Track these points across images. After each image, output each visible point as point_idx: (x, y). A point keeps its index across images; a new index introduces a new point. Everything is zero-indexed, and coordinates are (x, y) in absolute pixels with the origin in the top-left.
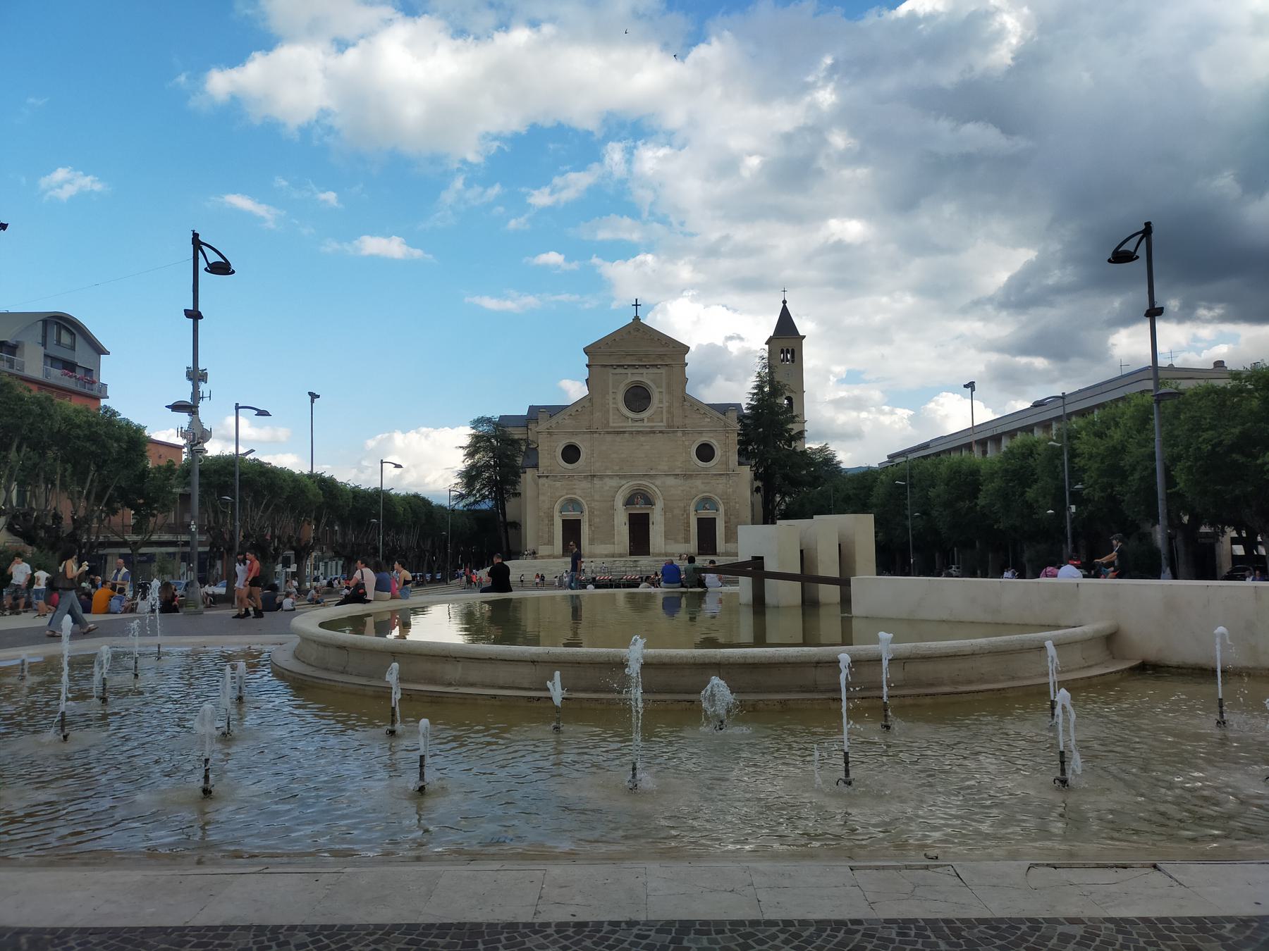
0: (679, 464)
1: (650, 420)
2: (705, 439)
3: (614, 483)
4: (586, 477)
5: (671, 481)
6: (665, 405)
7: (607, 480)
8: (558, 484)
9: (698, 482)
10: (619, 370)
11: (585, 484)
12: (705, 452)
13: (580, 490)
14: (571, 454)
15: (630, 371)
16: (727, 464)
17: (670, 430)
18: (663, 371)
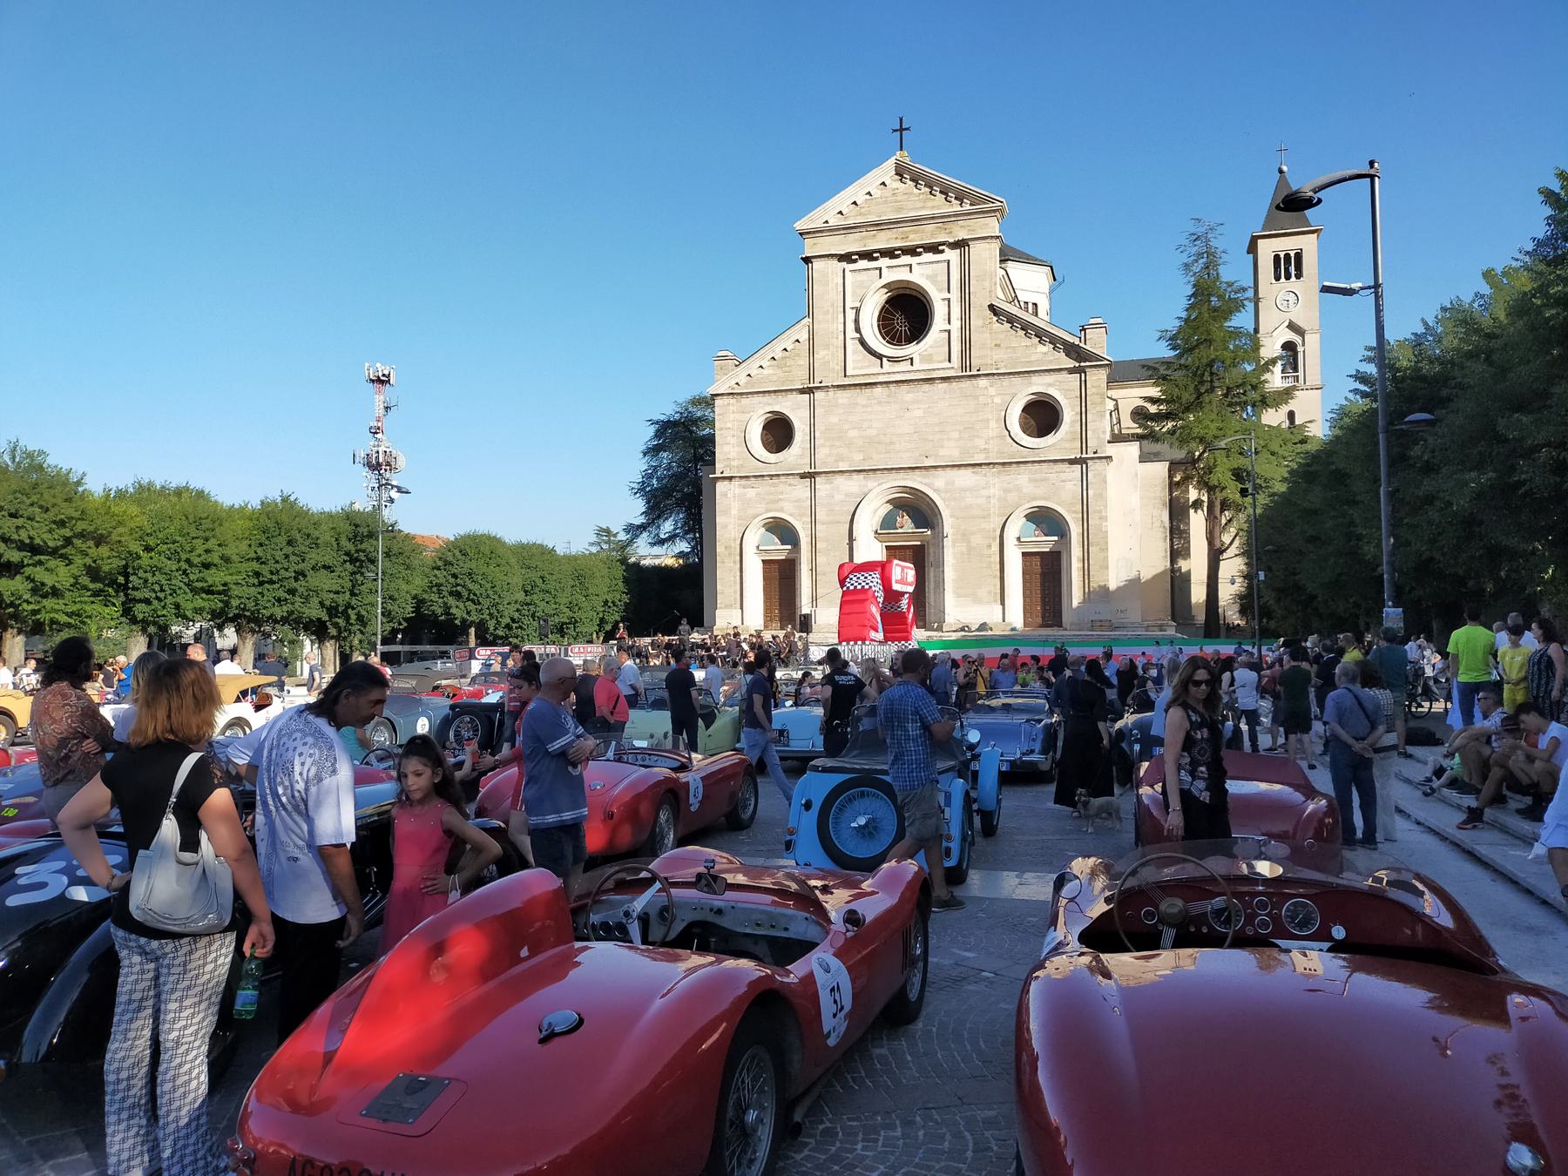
0: (980, 443)
1: (927, 358)
2: (1040, 385)
3: (853, 484)
4: (803, 476)
5: (965, 478)
6: (956, 326)
7: (839, 479)
8: (751, 493)
9: (1022, 479)
10: (863, 264)
11: (802, 489)
12: (1042, 416)
13: (791, 503)
14: (778, 433)
15: (884, 262)
16: (1084, 440)
17: (968, 373)
18: (952, 255)
